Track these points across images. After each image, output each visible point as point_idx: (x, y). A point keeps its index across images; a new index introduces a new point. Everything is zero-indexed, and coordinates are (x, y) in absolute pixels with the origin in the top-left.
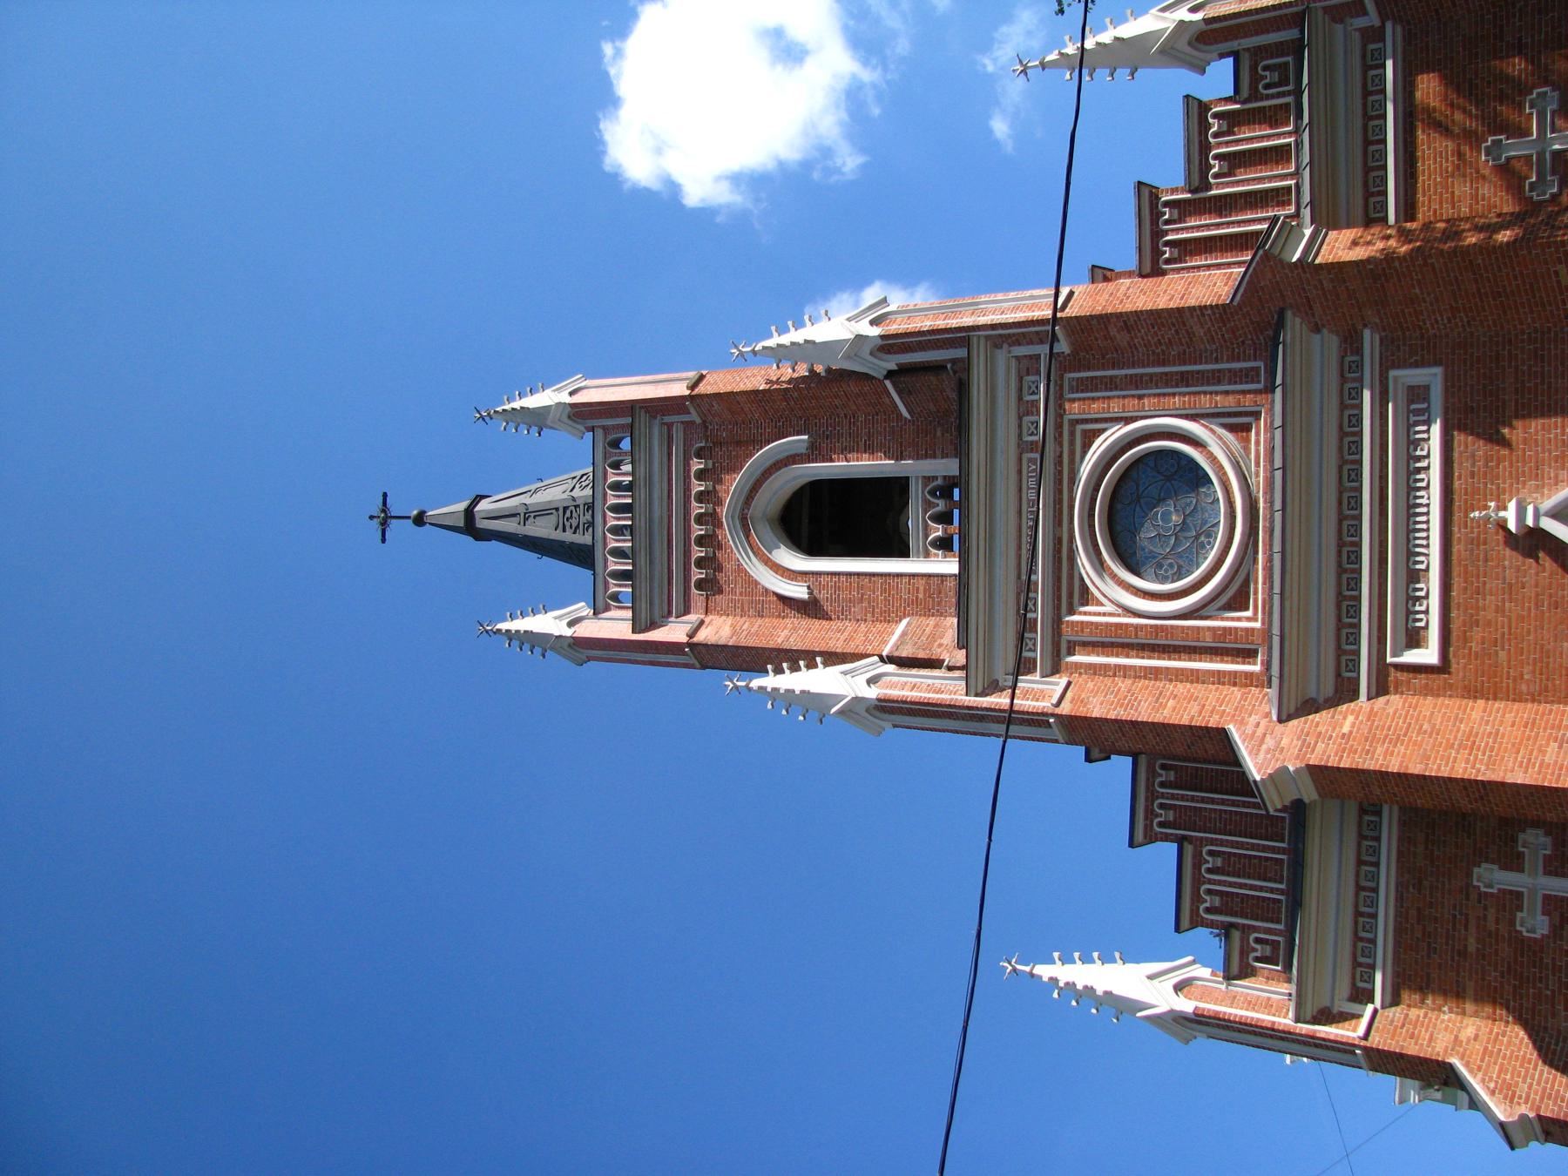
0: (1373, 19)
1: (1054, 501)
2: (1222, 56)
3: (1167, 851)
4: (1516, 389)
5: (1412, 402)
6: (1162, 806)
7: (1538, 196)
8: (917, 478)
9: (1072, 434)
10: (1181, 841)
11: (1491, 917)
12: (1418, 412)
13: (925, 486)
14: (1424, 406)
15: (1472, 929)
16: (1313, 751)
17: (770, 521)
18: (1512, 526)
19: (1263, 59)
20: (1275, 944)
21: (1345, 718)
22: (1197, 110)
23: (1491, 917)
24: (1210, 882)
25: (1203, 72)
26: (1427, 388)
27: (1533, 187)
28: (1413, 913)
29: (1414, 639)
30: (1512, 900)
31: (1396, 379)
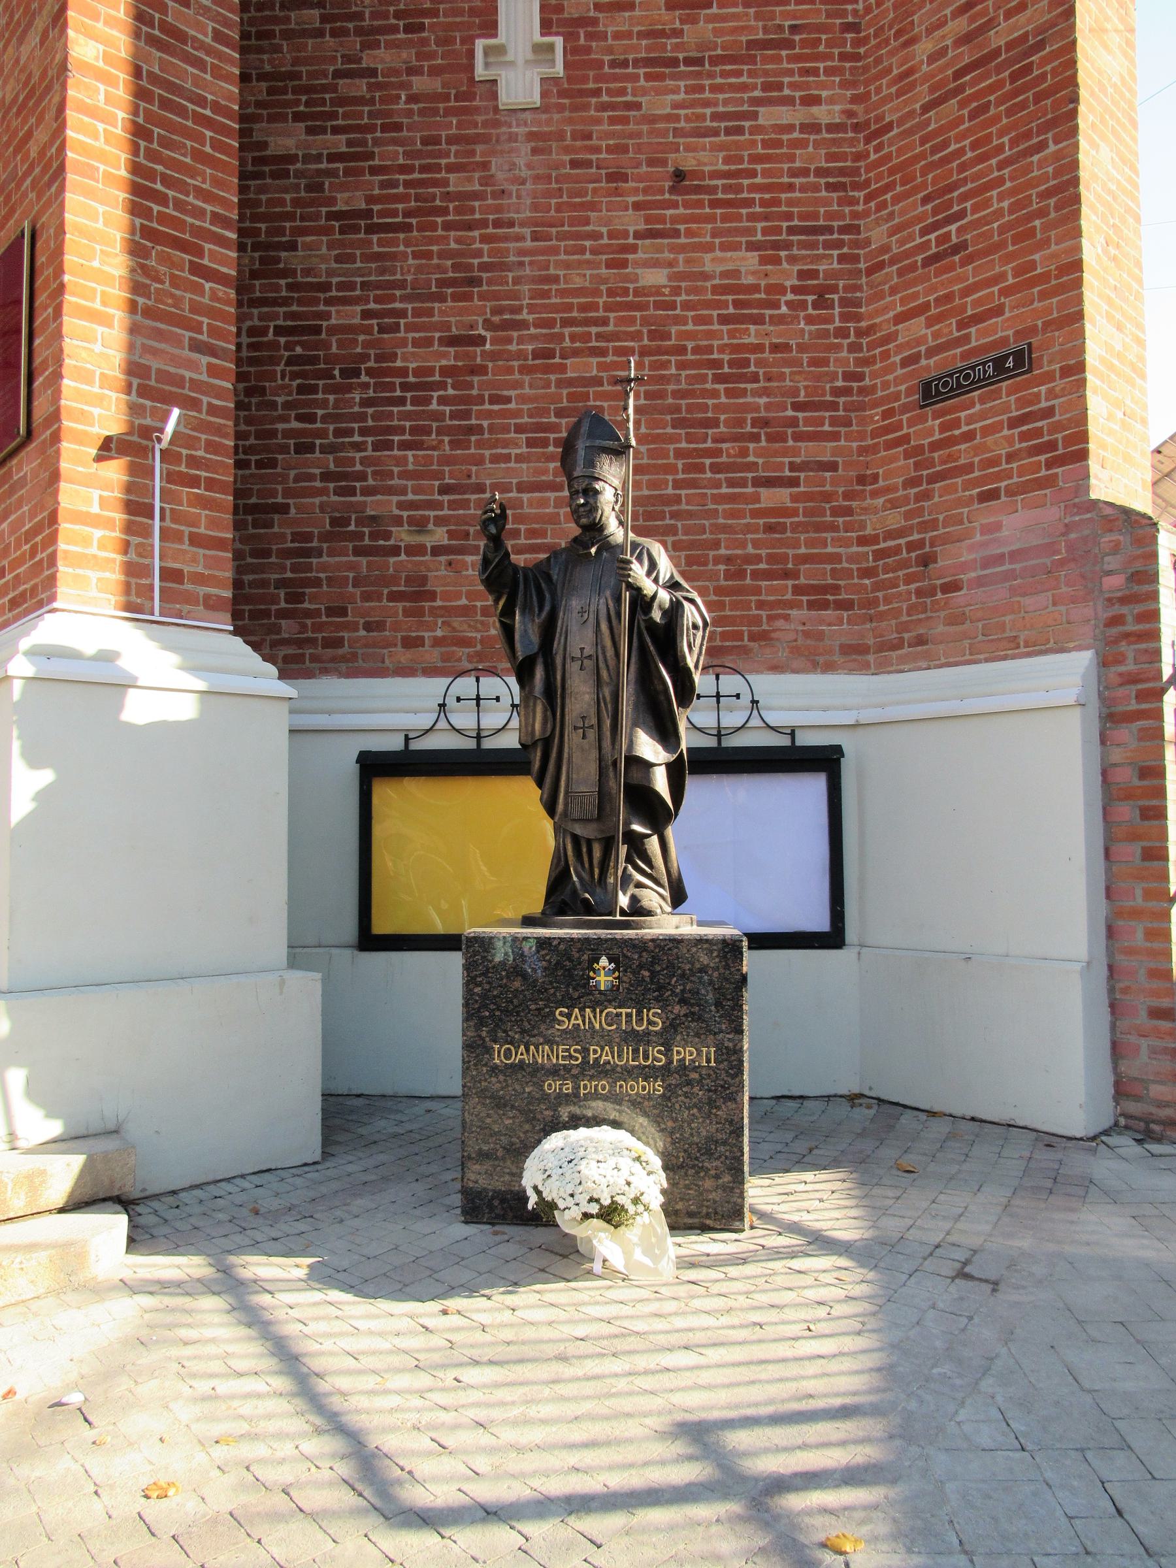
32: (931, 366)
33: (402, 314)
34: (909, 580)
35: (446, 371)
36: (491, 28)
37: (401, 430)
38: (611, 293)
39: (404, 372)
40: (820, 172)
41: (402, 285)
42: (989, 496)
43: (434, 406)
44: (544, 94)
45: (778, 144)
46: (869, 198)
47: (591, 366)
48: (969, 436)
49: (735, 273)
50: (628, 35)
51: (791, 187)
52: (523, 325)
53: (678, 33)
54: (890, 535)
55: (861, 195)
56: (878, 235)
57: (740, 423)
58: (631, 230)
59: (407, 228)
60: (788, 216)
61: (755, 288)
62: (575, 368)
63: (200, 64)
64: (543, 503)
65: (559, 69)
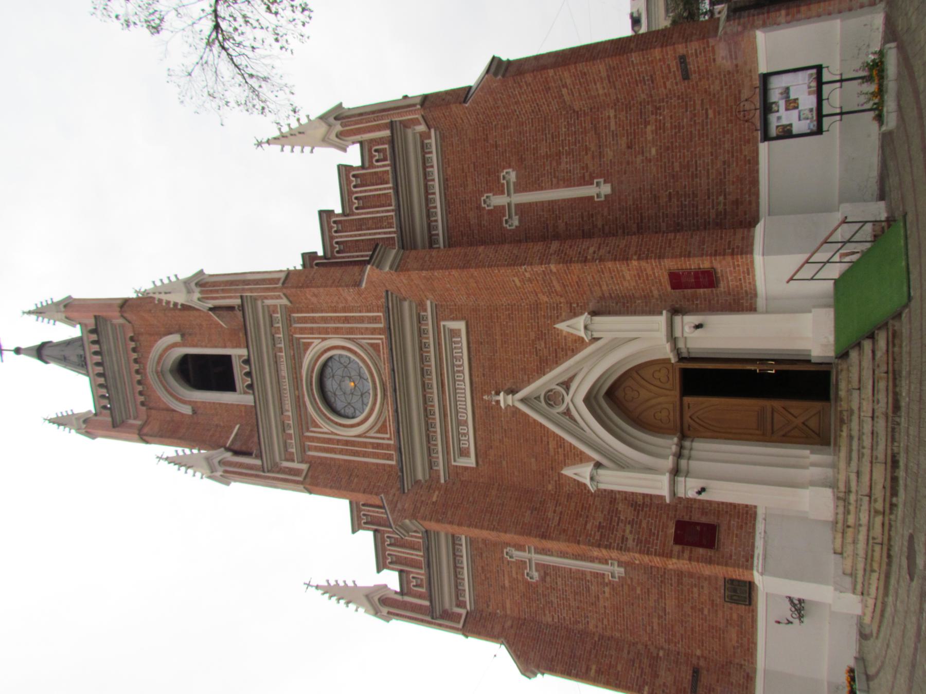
0: (422, 128)
1: (293, 378)
2: (354, 143)
3: (366, 537)
4: (501, 334)
5: (454, 337)
6: (364, 515)
7: (510, 226)
8: (235, 355)
9: (299, 344)
10: (376, 531)
11: (514, 573)
12: (456, 343)
13: (239, 359)
14: (459, 339)
15: (506, 576)
16: (419, 512)
17: (171, 371)
18: (502, 404)
19: (374, 145)
20: (422, 580)
21: (434, 492)
22: (344, 171)
23: (514, 573)
24: (389, 550)
25: (345, 150)
26: (459, 330)
27: (507, 221)
28: (480, 568)
29: (464, 453)
30: (521, 564)
31: (444, 326)
32: (679, 78)
33: (663, 213)
34: (733, 76)
35: (678, 200)
36: (592, 197)
37: (693, 211)
38: (658, 161)
39: (678, 211)
40: (627, 113)
41: (656, 213)
42: (714, 60)
43: (687, 203)
44: (608, 182)
45: (620, 125)
46: (633, 99)
47: (677, 165)
48: (698, 67)
49: (652, 131)
50: (594, 165)
51: (630, 120)
52: (666, 183)
53: (593, 152)
54: (721, 82)
55: (632, 102)
56: (643, 96)
57: (691, 125)
58: (641, 158)
59: (641, 213)
60: (637, 120)
61: (656, 126)
62: (677, 169)
63: (630, 242)
64: (712, 173)
65: (602, 180)
